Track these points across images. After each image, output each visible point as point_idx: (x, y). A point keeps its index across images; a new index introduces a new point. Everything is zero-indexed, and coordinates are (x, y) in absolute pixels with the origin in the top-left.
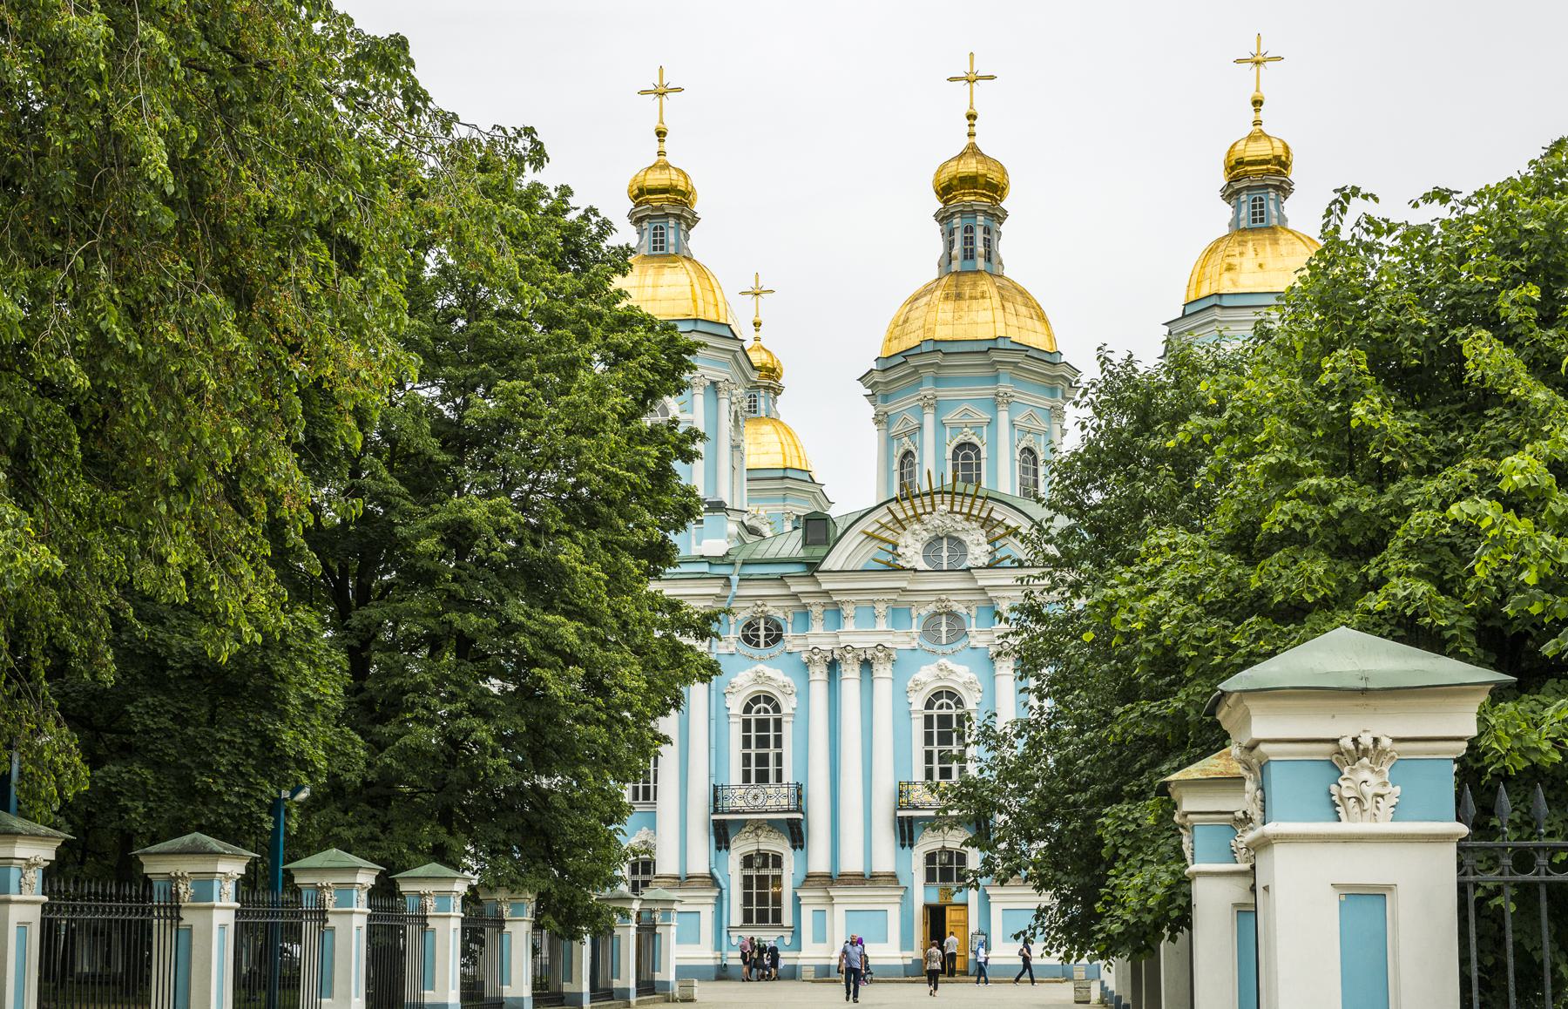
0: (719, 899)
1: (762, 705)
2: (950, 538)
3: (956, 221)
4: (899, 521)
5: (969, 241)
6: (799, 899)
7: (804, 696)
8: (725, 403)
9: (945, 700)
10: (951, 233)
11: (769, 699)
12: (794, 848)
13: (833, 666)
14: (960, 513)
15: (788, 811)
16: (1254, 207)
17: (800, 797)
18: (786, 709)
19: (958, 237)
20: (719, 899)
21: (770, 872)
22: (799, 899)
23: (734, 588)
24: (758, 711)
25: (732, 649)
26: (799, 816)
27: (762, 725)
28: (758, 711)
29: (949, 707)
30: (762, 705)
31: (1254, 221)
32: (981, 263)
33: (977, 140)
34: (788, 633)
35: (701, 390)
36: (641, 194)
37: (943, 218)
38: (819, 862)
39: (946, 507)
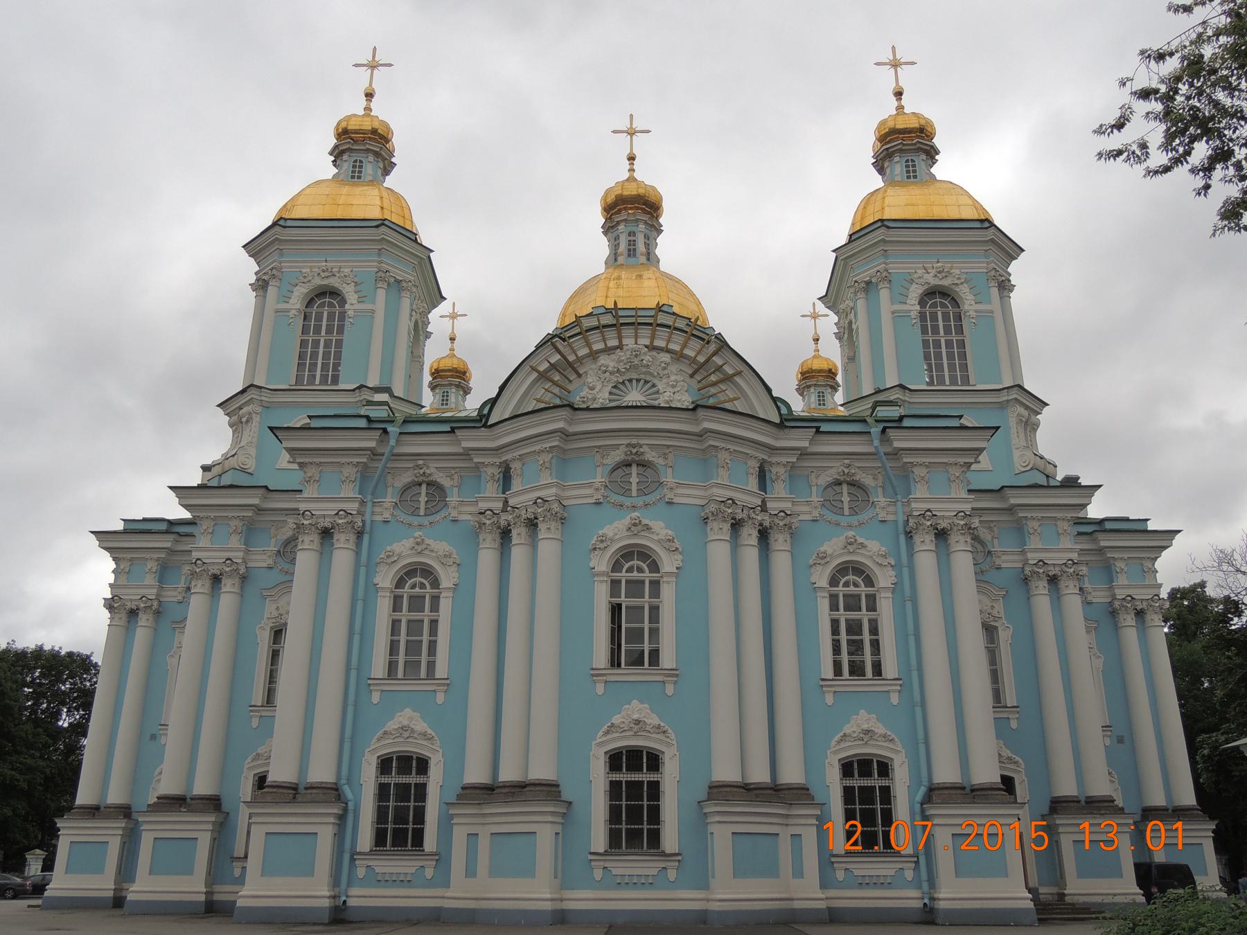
0: (342, 818)
1: (418, 579)
3: (621, 227)
5: (632, 244)
6: (452, 817)
7: (467, 567)
8: (406, 303)
10: (617, 238)
11: (427, 572)
13: (505, 534)
16: (907, 166)
18: (446, 582)
20: (342, 818)
21: (413, 779)
23: (392, 442)
24: (413, 587)
25: (387, 515)
28: (413, 587)
31: (908, 177)
32: (643, 259)
33: (636, 175)
34: (453, 498)
36: (344, 133)
37: (608, 229)
38: (476, 774)
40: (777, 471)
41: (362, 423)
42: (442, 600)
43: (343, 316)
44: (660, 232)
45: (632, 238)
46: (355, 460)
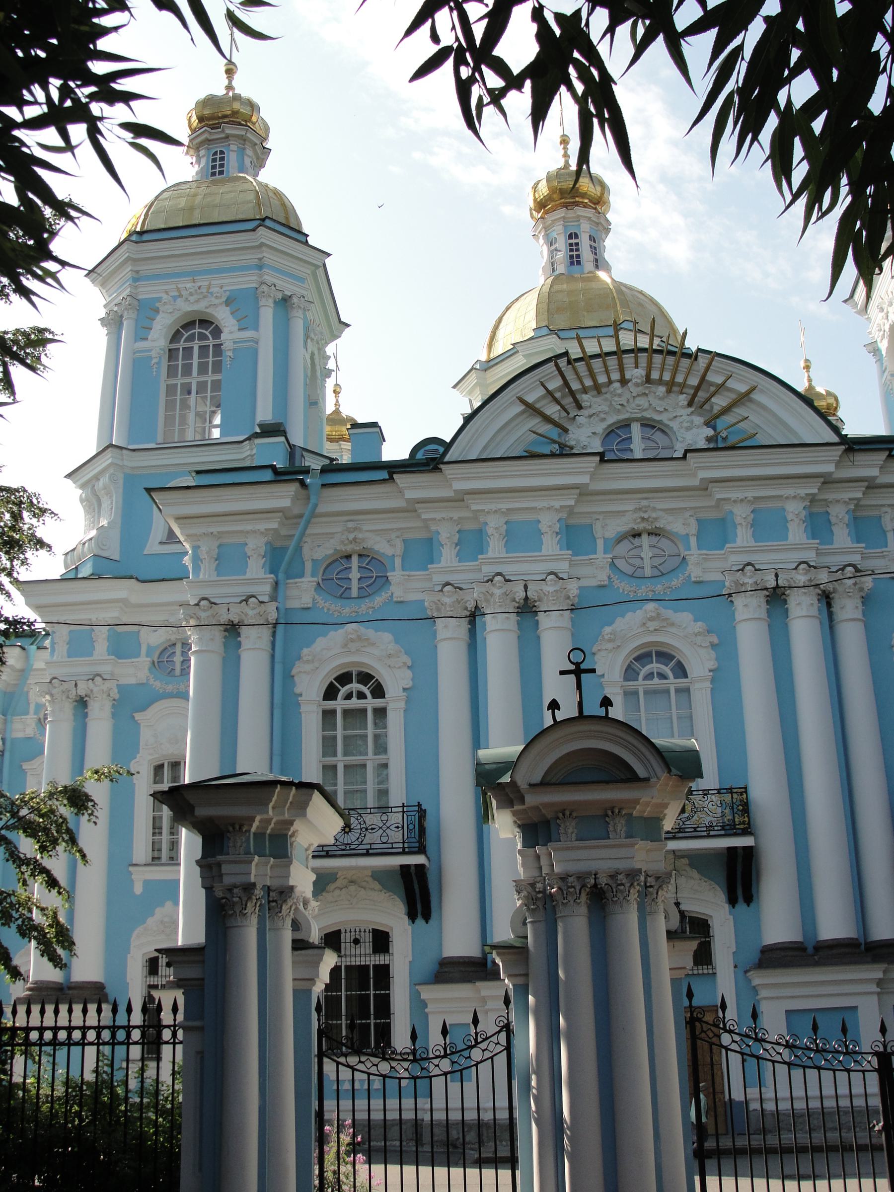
1: (355, 686)
2: (648, 424)
4: (572, 393)
6: (424, 1004)
9: (655, 666)
12: (412, 916)
13: (474, 616)
14: (660, 382)
15: (404, 853)
17: (422, 830)
19: (562, 243)
22: (755, 990)
26: (420, 859)
27: (354, 716)
28: (349, 696)
29: (662, 676)
30: (355, 686)
34: (396, 576)
35: (270, 302)
39: (641, 372)
40: (839, 513)
41: (268, 475)
42: (390, 714)
43: (218, 348)
44: (608, 231)
45: (574, 241)
46: (262, 526)
